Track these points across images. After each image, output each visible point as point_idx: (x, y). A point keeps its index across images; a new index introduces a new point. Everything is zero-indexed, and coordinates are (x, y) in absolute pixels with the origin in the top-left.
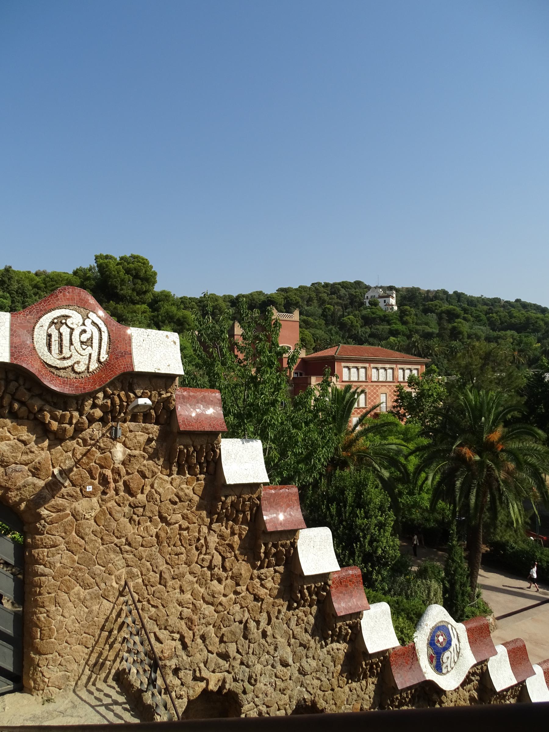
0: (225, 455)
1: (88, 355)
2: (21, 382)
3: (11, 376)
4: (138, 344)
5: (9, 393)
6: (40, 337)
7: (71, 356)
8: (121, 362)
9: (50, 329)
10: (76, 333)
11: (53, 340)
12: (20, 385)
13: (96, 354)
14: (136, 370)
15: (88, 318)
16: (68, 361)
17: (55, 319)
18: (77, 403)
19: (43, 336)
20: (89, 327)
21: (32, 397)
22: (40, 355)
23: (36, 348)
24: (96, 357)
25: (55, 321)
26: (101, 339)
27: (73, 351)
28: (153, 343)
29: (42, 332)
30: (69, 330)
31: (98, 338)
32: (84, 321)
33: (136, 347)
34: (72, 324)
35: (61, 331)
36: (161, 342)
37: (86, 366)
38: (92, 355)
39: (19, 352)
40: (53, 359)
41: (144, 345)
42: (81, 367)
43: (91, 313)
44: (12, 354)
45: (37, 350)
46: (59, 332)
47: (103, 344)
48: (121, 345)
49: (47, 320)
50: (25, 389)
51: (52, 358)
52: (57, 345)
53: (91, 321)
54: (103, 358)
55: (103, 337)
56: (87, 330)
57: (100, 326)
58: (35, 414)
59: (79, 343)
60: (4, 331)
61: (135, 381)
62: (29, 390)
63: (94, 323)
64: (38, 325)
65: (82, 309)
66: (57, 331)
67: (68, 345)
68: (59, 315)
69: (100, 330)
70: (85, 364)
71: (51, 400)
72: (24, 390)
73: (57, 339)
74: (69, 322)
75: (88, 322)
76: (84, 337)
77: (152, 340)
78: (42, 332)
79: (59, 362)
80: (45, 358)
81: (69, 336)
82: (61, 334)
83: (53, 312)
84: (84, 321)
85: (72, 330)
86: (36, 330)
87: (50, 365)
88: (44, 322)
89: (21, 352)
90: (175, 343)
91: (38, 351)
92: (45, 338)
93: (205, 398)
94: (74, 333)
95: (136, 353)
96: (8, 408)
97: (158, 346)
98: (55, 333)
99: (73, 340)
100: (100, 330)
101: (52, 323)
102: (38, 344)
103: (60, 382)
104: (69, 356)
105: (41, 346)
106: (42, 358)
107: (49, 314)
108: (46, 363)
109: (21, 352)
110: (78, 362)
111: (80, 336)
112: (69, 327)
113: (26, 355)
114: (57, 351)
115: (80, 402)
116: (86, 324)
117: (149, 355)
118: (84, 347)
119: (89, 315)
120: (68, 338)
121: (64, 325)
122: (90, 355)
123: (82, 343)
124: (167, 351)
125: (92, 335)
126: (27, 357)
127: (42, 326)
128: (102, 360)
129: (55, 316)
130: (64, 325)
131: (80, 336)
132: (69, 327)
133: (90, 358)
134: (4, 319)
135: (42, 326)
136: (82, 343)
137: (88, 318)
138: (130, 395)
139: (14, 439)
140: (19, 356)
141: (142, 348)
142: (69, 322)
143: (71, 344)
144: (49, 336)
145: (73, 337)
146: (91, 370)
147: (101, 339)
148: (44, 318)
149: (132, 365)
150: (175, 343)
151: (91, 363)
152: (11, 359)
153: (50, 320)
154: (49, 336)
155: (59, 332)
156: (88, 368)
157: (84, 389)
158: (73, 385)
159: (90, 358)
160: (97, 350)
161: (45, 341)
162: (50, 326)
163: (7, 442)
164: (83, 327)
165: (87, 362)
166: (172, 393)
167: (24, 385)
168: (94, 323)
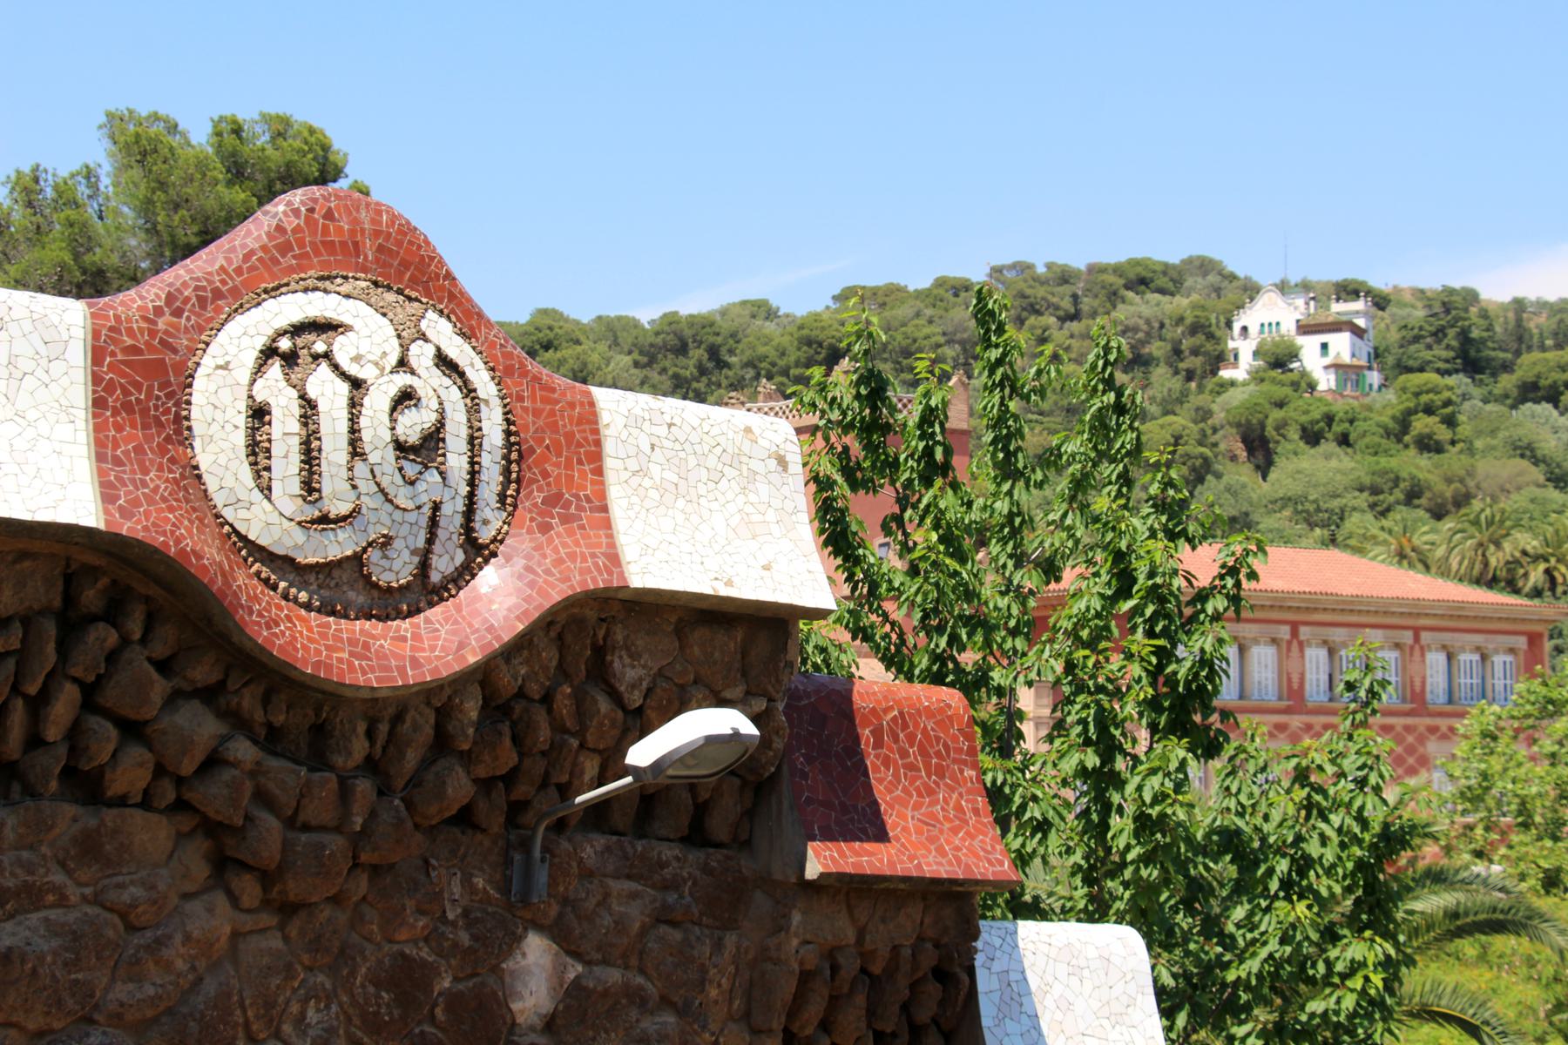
0: (996, 997)
1: (427, 511)
2: (136, 628)
3: (91, 597)
4: (633, 465)
5: (75, 680)
6: (218, 415)
7: (356, 511)
8: (565, 545)
9: (260, 383)
10: (377, 402)
11: (276, 430)
12: (125, 641)
13: (460, 505)
14: (636, 582)
15: (424, 337)
16: (342, 535)
17: (281, 333)
18: (370, 734)
19: (231, 413)
20: (429, 381)
21: (174, 698)
22: (219, 499)
23: (203, 467)
24: (459, 520)
25: (285, 344)
26: (474, 441)
27: (366, 486)
28: (692, 461)
29: (225, 396)
30: (344, 388)
31: (464, 432)
32: (405, 348)
33: (625, 475)
34: (357, 359)
35: (312, 393)
36: (726, 458)
37: (416, 560)
38: (446, 509)
39: (133, 481)
40: (270, 519)
41: (655, 470)
42: (397, 565)
43: (431, 315)
44: (108, 493)
45: (206, 477)
46: (303, 397)
47: (485, 459)
48: (558, 465)
49: (246, 341)
50: (149, 659)
51: (275, 518)
52: (296, 458)
53: (430, 351)
54: (486, 522)
55: (485, 425)
56: (421, 393)
57: (470, 374)
58: (180, 781)
59: (391, 454)
60: (65, 381)
61: (619, 635)
62: (163, 667)
63: (444, 362)
64: (208, 361)
65: (391, 297)
66: (294, 393)
67: (342, 457)
68: (297, 317)
69: (468, 390)
70: (414, 552)
71: (259, 716)
72: (146, 664)
73: (295, 426)
74: (343, 349)
75: (421, 355)
76: (413, 424)
77: (687, 446)
78: (225, 396)
79: (299, 536)
80: (243, 514)
81: (345, 415)
82: (309, 406)
83: (270, 304)
84: (405, 348)
85: (357, 384)
86: (199, 383)
87: (262, 549)
88: (233, 350)
89: (144, 484)
90: (782, 462)
91: (211, 484)
92: (242, 420)
93: (905, 726)
94: (366, 401)
95: (624, 503)
96: (62, 751)
97: (716, 477)
98: (283, 401)
99: (366, 435)
100: (468, 390)
101: (269, 352)
102: (212, 448)
103: (310, 630)
104: (344, 508)
105: (222, 460)
106: (228, 514)
107: (254, 314)
108: (243, 538)
109: (144, 484)
110: (387, 542)
111: (393, 420)
112: (344, 375)
113: (164, 499)
114: (295, 487)
115: (383, 728)
116: (414, 362)
117: (680, 518)
118: (411, 469)
119: (424, 325)
120: (343, 426)
121: (324, 367)
122: (436, 507)
123: (401, 447)
124: (752, 498)
125: (442, 412)
126: (171, 509)
127: (225, 367)
128: (485, 535)
129: (283, 322)
130: (324, 367)
131: (393, 420)
132: (344, 375)
133: (433, 522)
134: (62, 329)
135: (225, 367)
136: (401, 447)
137: (424, 337)
138: (596, 702)
139: (84, 898)
140: (136, 503)
141: (647, 483)
142: (343, 349)
143: (356, 450)
144: (259, 413)
145: (363, 422)
146: (435, 577)
147: (474, 441)
148: (233, 328)
149: (614, 559)
150: (782, 462)
151: (437, 547)
152: (107, 512)
153: (260, 342)
154: (259, 413)
155: (303, 397)
156: (424, 567)
157: (415, 663)
158: (366, 646)
159: (433, 522)
160: (464, 489)
161: (240, 439)
162: (259, 370)
163: (53, 914)
164: (403, 379)
165: (421, 543)
166: (771, 700)
167: (144, 641)
168: (444, 362)
